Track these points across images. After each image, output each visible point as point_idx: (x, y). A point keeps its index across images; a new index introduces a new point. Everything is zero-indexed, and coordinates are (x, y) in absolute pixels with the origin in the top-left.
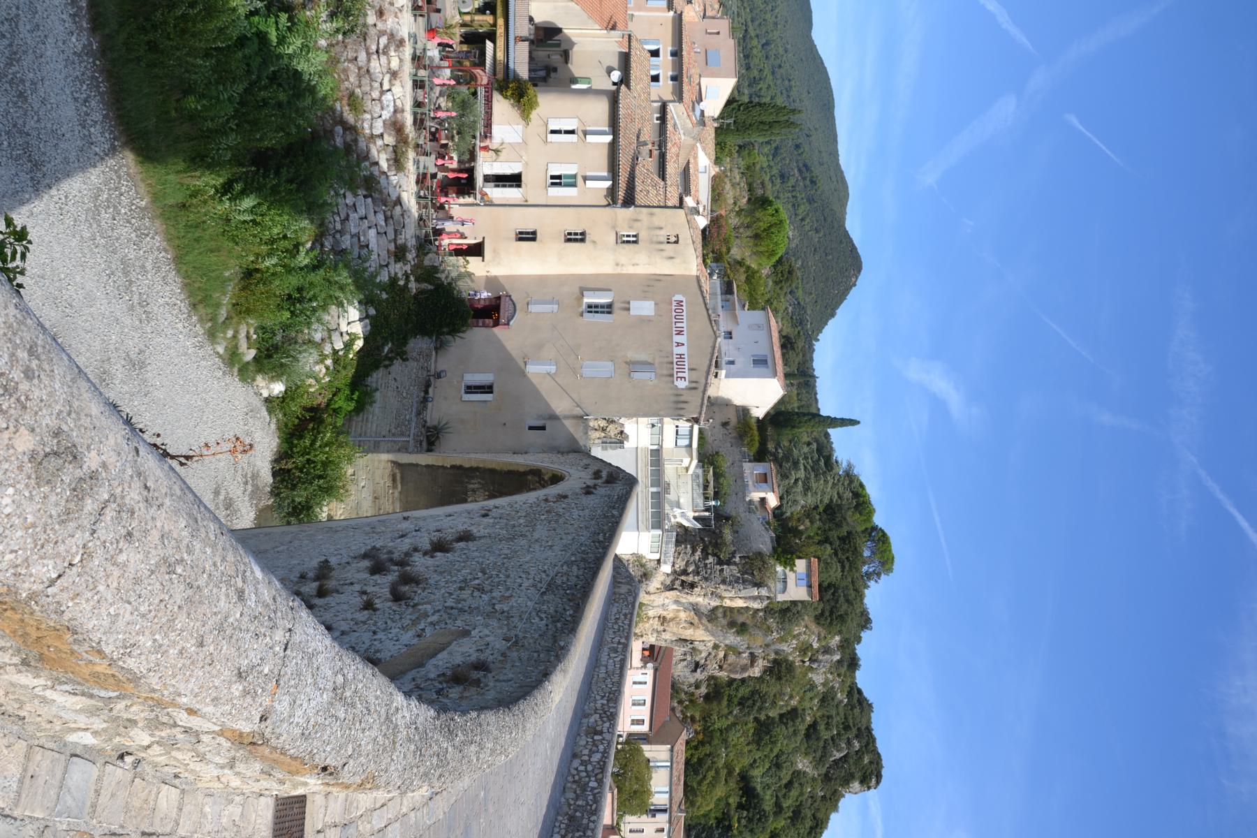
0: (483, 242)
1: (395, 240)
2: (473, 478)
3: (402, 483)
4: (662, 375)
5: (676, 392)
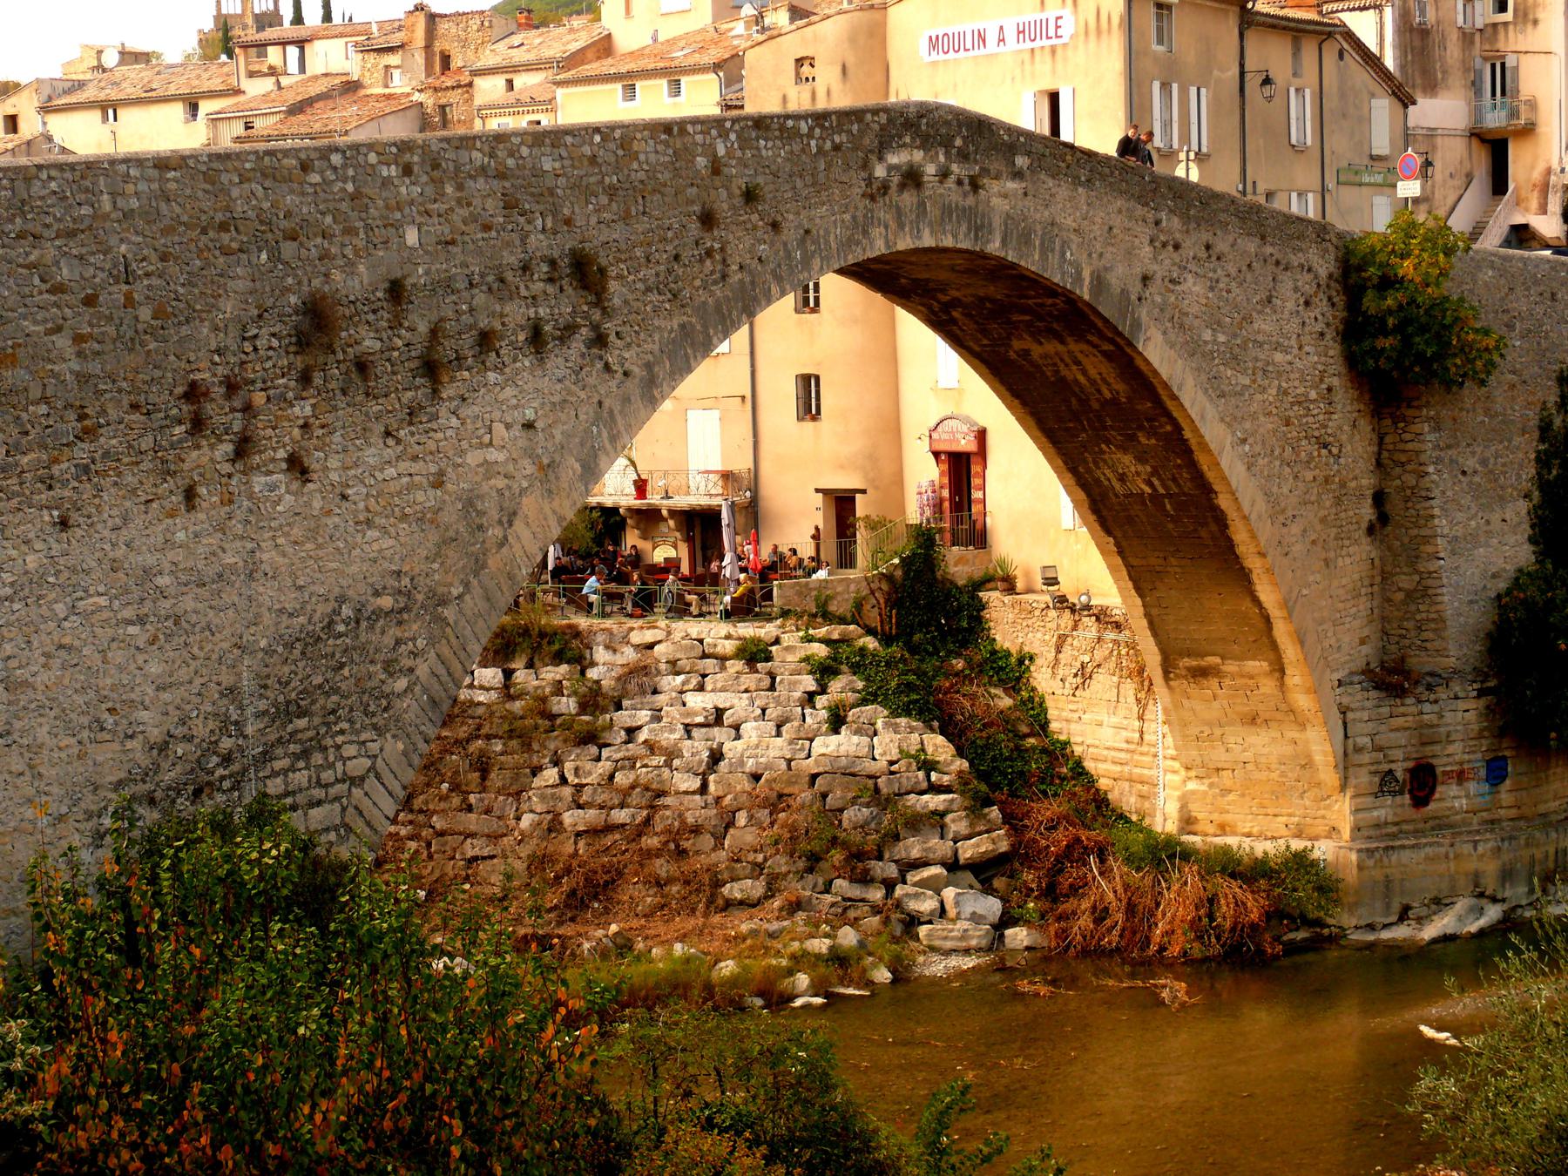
0: (825, 492)
1: (723, 659)
2: (1098, 481)
3: (1203, 655)
4: (1054, 72)
5: (1082, 37)
